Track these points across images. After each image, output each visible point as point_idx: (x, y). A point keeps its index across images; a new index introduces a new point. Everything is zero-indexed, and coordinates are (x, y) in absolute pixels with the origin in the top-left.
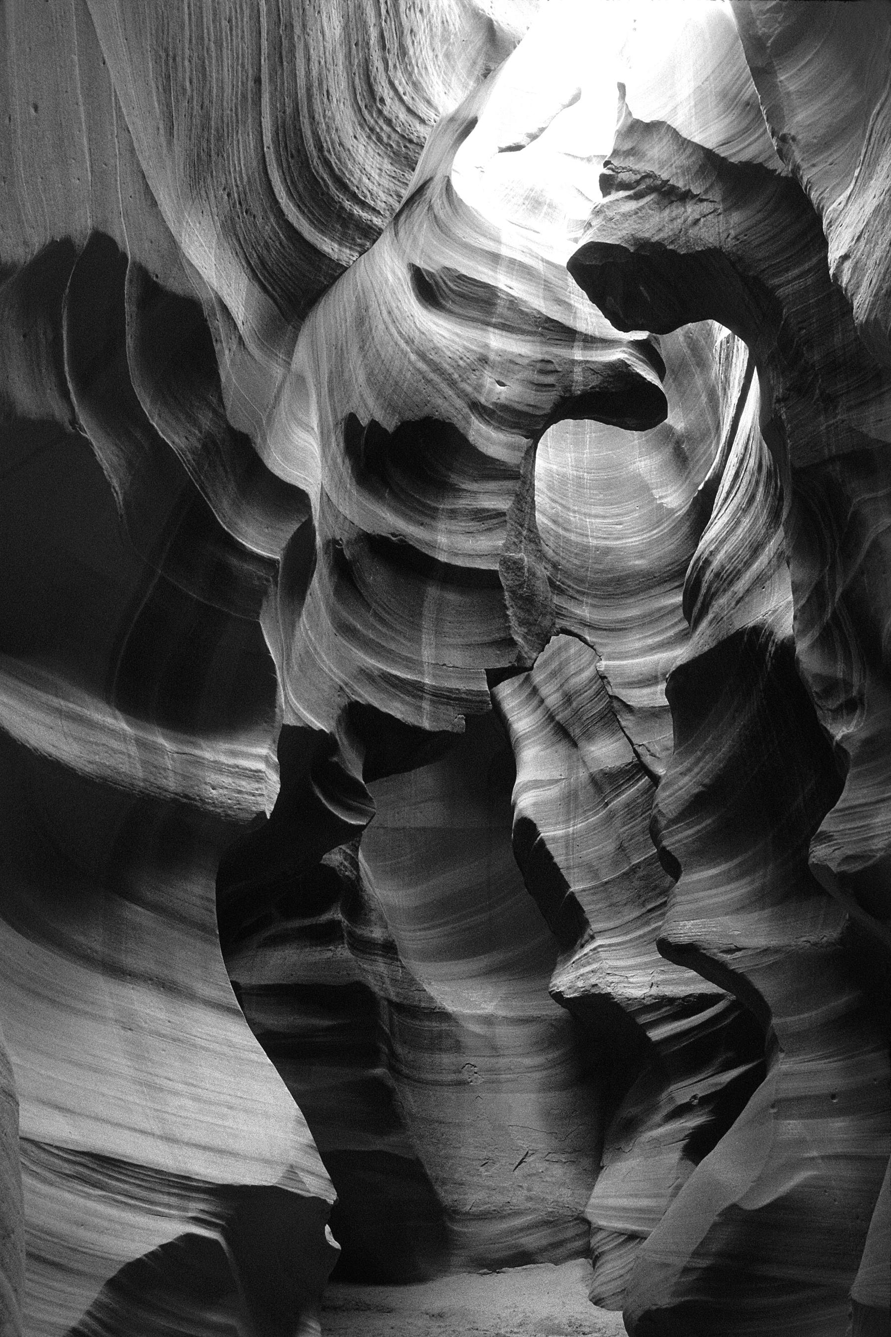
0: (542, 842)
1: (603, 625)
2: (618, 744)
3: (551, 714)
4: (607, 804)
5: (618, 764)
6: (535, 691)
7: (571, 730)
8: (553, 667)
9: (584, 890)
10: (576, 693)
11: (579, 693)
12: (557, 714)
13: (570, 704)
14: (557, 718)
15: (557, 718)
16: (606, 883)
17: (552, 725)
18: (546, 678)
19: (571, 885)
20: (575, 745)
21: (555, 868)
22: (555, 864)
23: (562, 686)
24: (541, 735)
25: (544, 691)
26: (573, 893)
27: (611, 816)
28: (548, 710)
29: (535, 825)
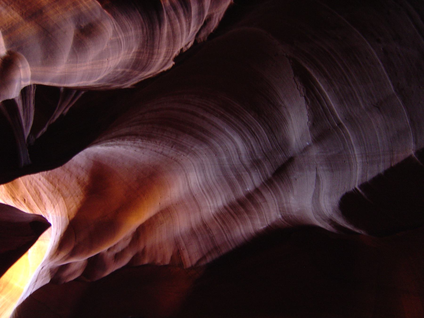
2: (292, 115)
4: (340, 124)
5: (306, 112)
6: (249, 196)
8: (234, 177)
9: (416, 142)
10: (252, 156)
11: (252, 153)
12: (267, 175)
15: (270, 176)
16: (411, 120)
17: (276, 183)
19: (409, 154)
20: (291, 160)
21: (390, 172)
22: (386, 172)
23: (247, 170)
24: (280, 190)
25: (249, 188)
26: (417, 152)
27: (350, 119)
28: (263, 185)
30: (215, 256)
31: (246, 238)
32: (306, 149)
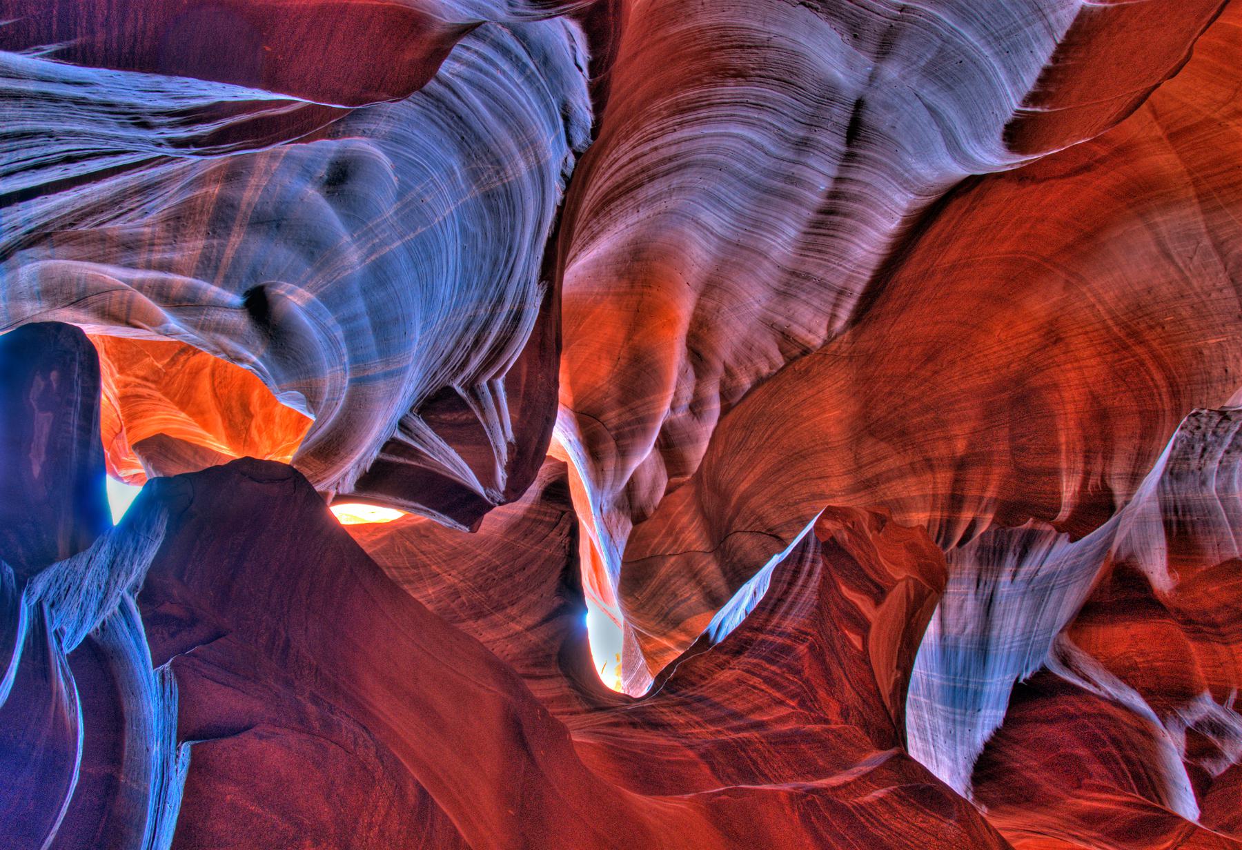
0: (1033, 99)
1: (539, 197)
3: (844, 160)
5: (825, 25)
6: (833, 195)
7: (845, 122)
8: (783, 184)
10: (787, 140)
11: (783, 137)
12: (837, 151)
13: (803, 138)
14: (843, 149)
15: (843, 149)
18: (804, 187)
20: (859, 104)
22: (1054, 59)
25: (824, 185)
28: (842, 167)
29: (1007, 126)
30: (849, 305)
31: (880, 252)
32: (873, 78)
